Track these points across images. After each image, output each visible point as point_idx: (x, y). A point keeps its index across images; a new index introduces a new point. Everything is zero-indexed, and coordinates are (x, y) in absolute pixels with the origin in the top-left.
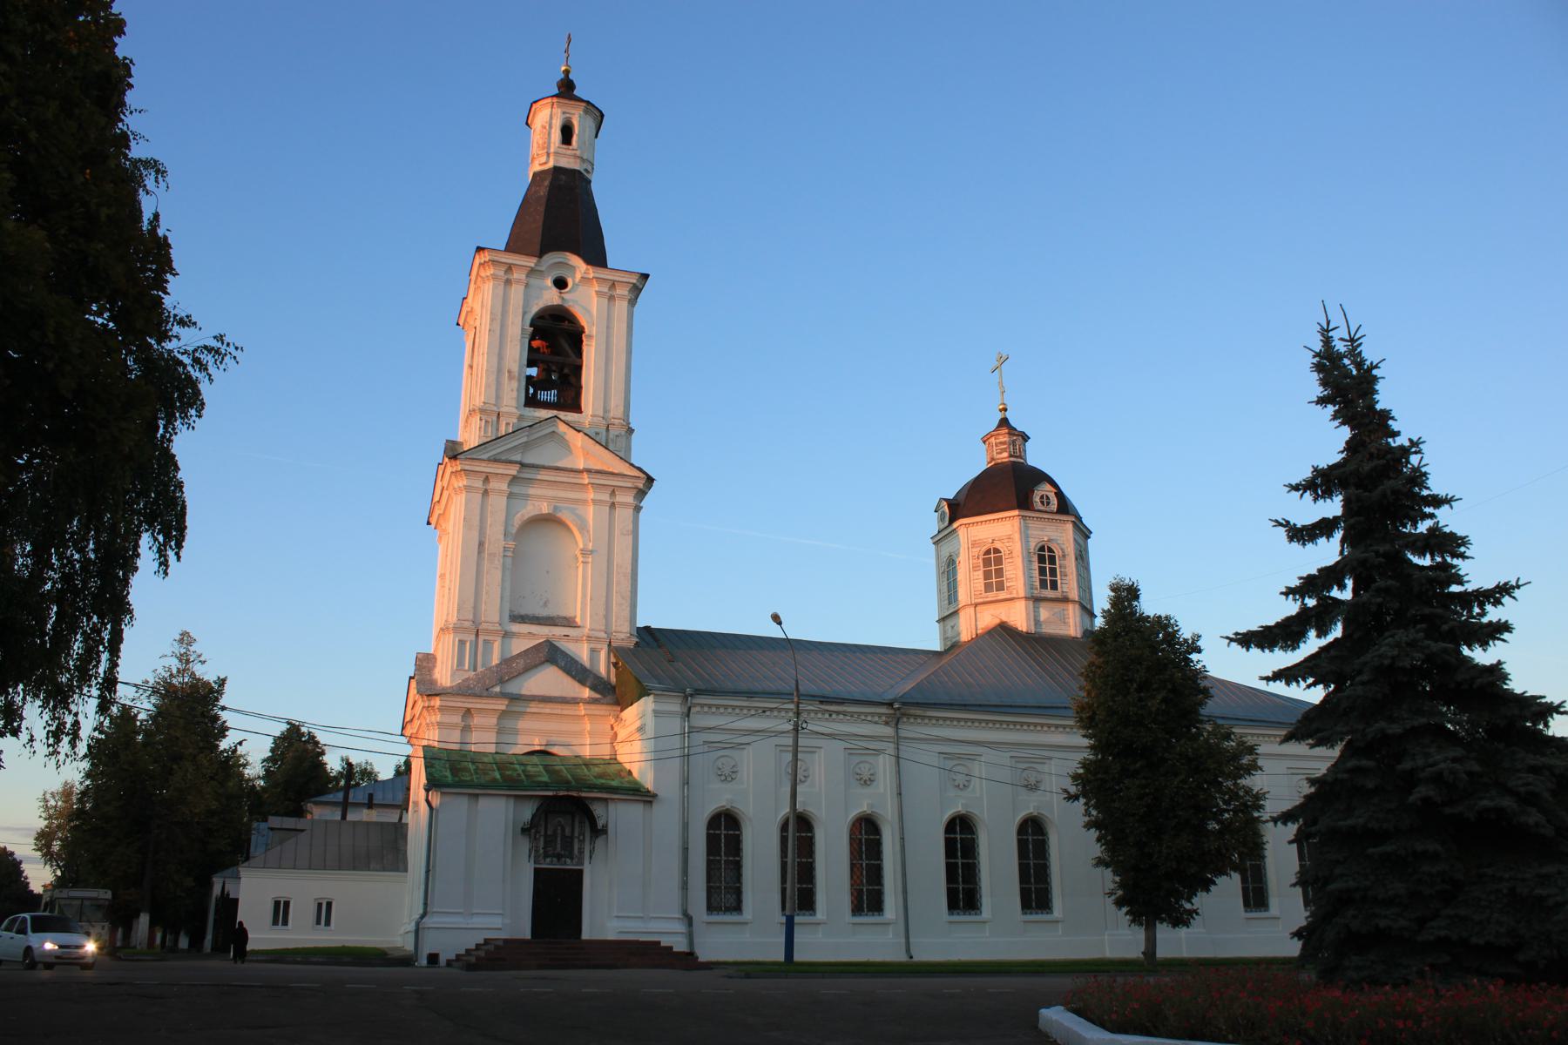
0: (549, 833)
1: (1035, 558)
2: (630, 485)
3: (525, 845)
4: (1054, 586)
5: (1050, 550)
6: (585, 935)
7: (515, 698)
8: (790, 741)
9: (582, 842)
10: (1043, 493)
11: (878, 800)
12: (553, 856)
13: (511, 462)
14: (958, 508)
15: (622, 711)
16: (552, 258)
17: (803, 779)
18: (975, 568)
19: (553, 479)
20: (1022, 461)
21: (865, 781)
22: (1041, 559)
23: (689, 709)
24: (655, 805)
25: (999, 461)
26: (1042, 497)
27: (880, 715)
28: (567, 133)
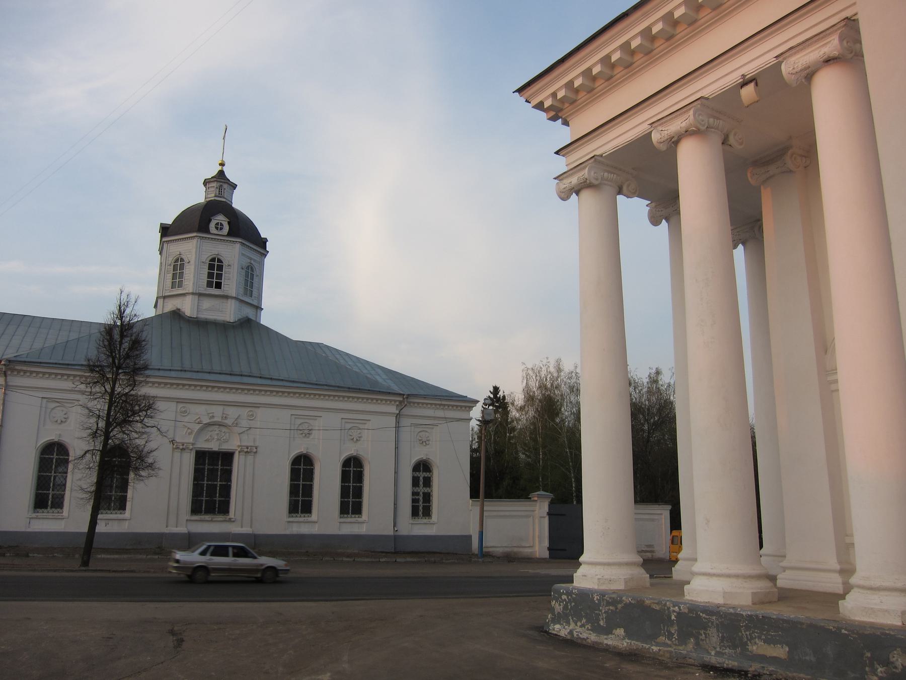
1: (207, 267)
4: (218, 286)
5: (220, 261)
10: (218, 221)
20: (224, 200)
22: (211, 267)
26: (217, 224)
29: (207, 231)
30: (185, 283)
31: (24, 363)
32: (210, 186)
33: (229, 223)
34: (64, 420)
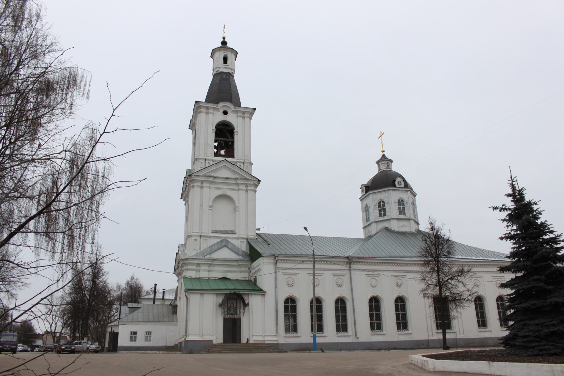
0: (229, 306)
1: (397, 204)
2: (252, 183)
3: (220, 311)
4: (404, 214)
5: (402, 201)
6: (242, 342)
7: (214, 260)
8: (312, 272)
9: (240, 309)
11: (344, 293)
12: (230, 314)
13: (210, 176)
14: (368, 188)
15: (252, 263)
16: (221, 104)
17: (317, 285)
18: (376, 209)
21: (340, 285)
22: (399, 204)
23: (277, 261)
24: (265, 296)
25: (382, 170)
26: (398, 182)
27: (344, 262)
28: (225, 60)
30: (387, 214)
31: (357, 258)
34: (374, 286)
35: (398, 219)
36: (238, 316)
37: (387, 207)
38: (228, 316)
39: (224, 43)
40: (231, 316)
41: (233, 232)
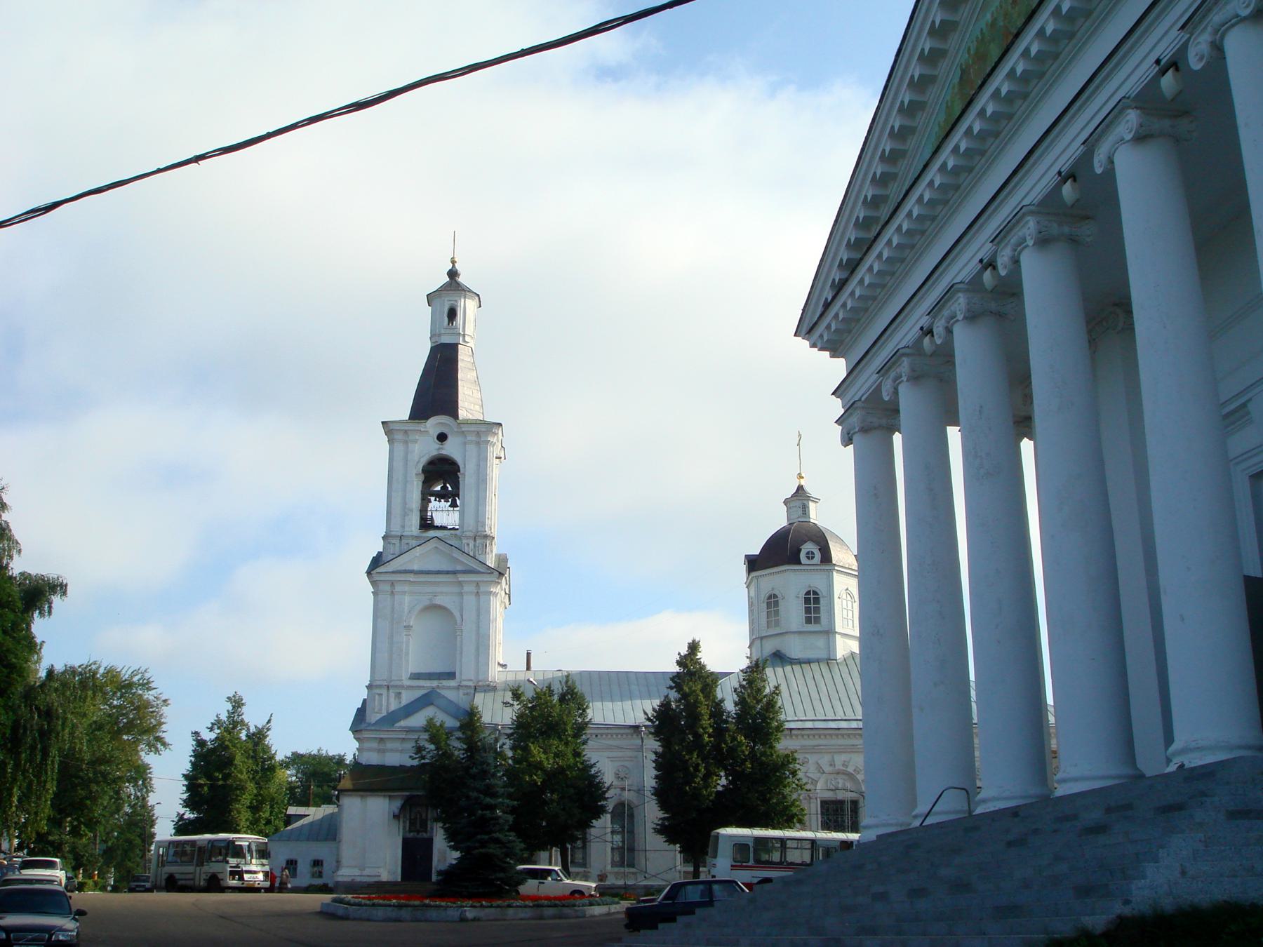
0: (413, 817)
4: (817, 620)
5: (815, 593)
14: (753, 564)
16: (433, 421)
19: (433, 580)
22: (807, 601)
26: (808, 553)
29: (799, 563)
32: (791, 505)
33: (820, 550)
35: (800, 633)
36: (428, 834)
37: (781, 603)
38: (412, 834)
39: (453, 274)
40: (415, 834)
41: (451, 675)
